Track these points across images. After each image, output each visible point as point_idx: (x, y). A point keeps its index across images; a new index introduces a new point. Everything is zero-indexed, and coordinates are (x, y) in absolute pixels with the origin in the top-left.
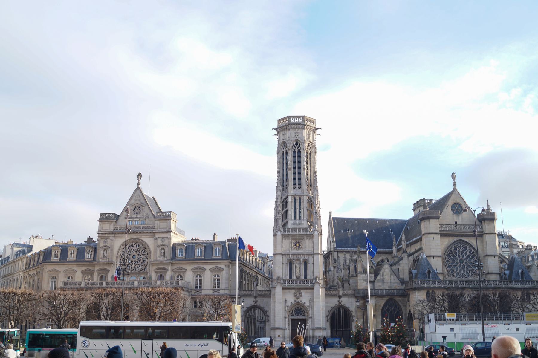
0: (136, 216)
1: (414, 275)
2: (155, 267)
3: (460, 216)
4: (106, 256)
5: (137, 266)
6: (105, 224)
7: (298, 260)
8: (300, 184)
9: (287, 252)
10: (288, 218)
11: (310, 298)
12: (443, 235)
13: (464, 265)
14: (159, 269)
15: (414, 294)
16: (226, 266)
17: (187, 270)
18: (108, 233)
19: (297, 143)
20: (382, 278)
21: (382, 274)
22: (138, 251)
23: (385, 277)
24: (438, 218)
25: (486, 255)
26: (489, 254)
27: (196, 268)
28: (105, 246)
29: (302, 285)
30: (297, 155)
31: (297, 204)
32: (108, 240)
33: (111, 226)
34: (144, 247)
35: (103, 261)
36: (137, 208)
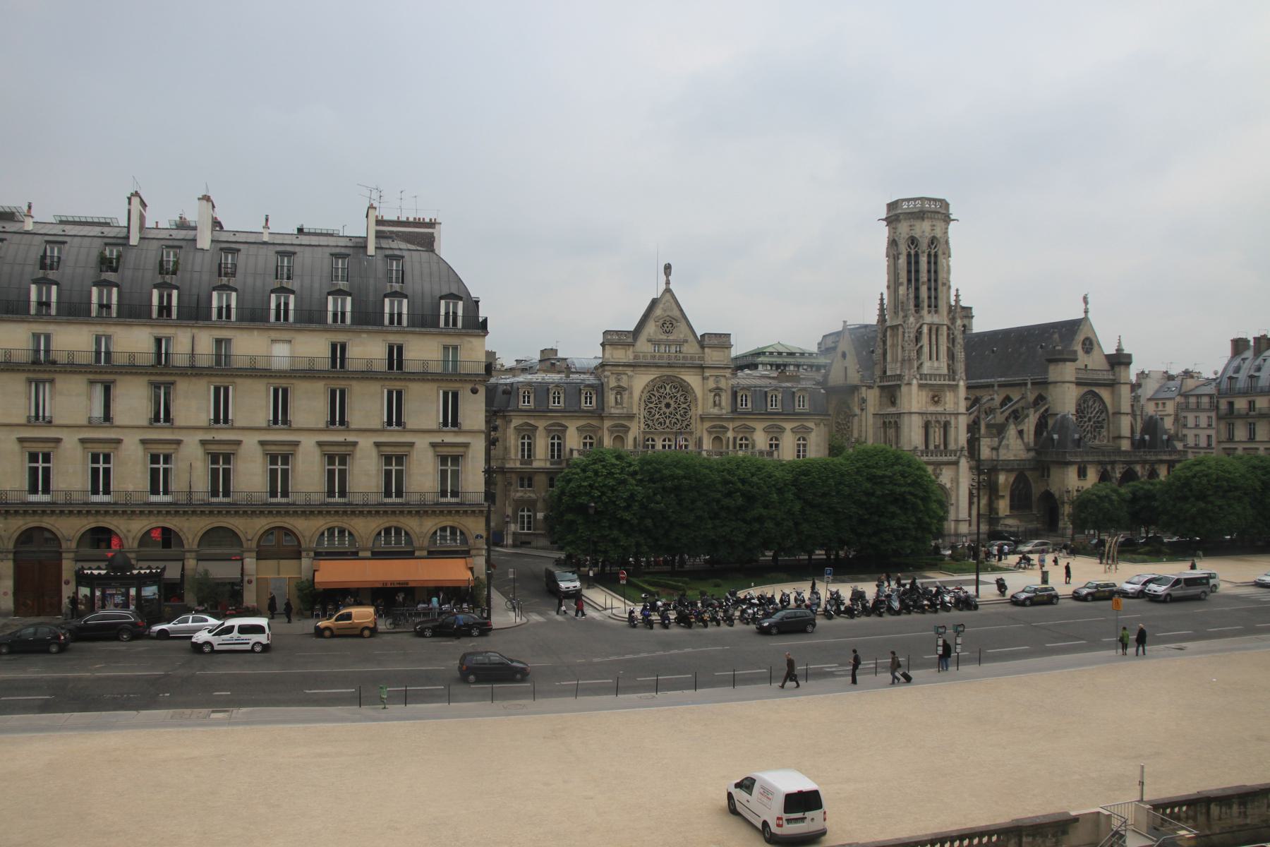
0: (666, 338)
1: (1056, 442)
2: (707, 425)
4: (621, 404)
5: (674, 420)
6: (617, 349)
7: (938, 422)
8: (936, 307)
9: (924, 410)
10: (923, 357)
11: (952, 478)
12: (1079, 383)
13: (1091, 426)
14: (714, 427)
16: (816, 424)
17: (755, 429)
18: (625, 365)
19: (933, 241)
20: (1007, 442)
22: (675, 396)
24: (1074, 360)
25: (1120, 413)
26: (1122, 411)
27: (771, 427)
28: (619, 387)
29: (944, 459)
30: (934, 260)
31: (934, 337)
32: (623, 376)
33: (628, 352)
34: (685, 389)
35: (617, 411)
36: (668, 323)
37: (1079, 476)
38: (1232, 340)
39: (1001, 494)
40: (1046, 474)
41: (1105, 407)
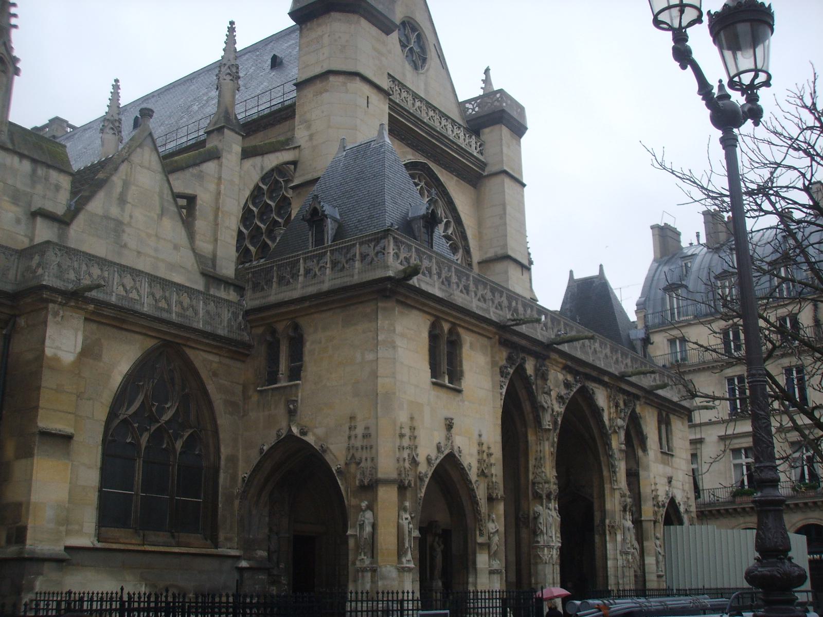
3: (422, 77)
15: (382, 322)
20: (115, 211)
21: (118, 189)
23: (131, 217)
26: (510, 253)
37: (435, 372)
38: (652, 228)
39: (48, 421)
40: (283, 366)
41: (464, 237)
